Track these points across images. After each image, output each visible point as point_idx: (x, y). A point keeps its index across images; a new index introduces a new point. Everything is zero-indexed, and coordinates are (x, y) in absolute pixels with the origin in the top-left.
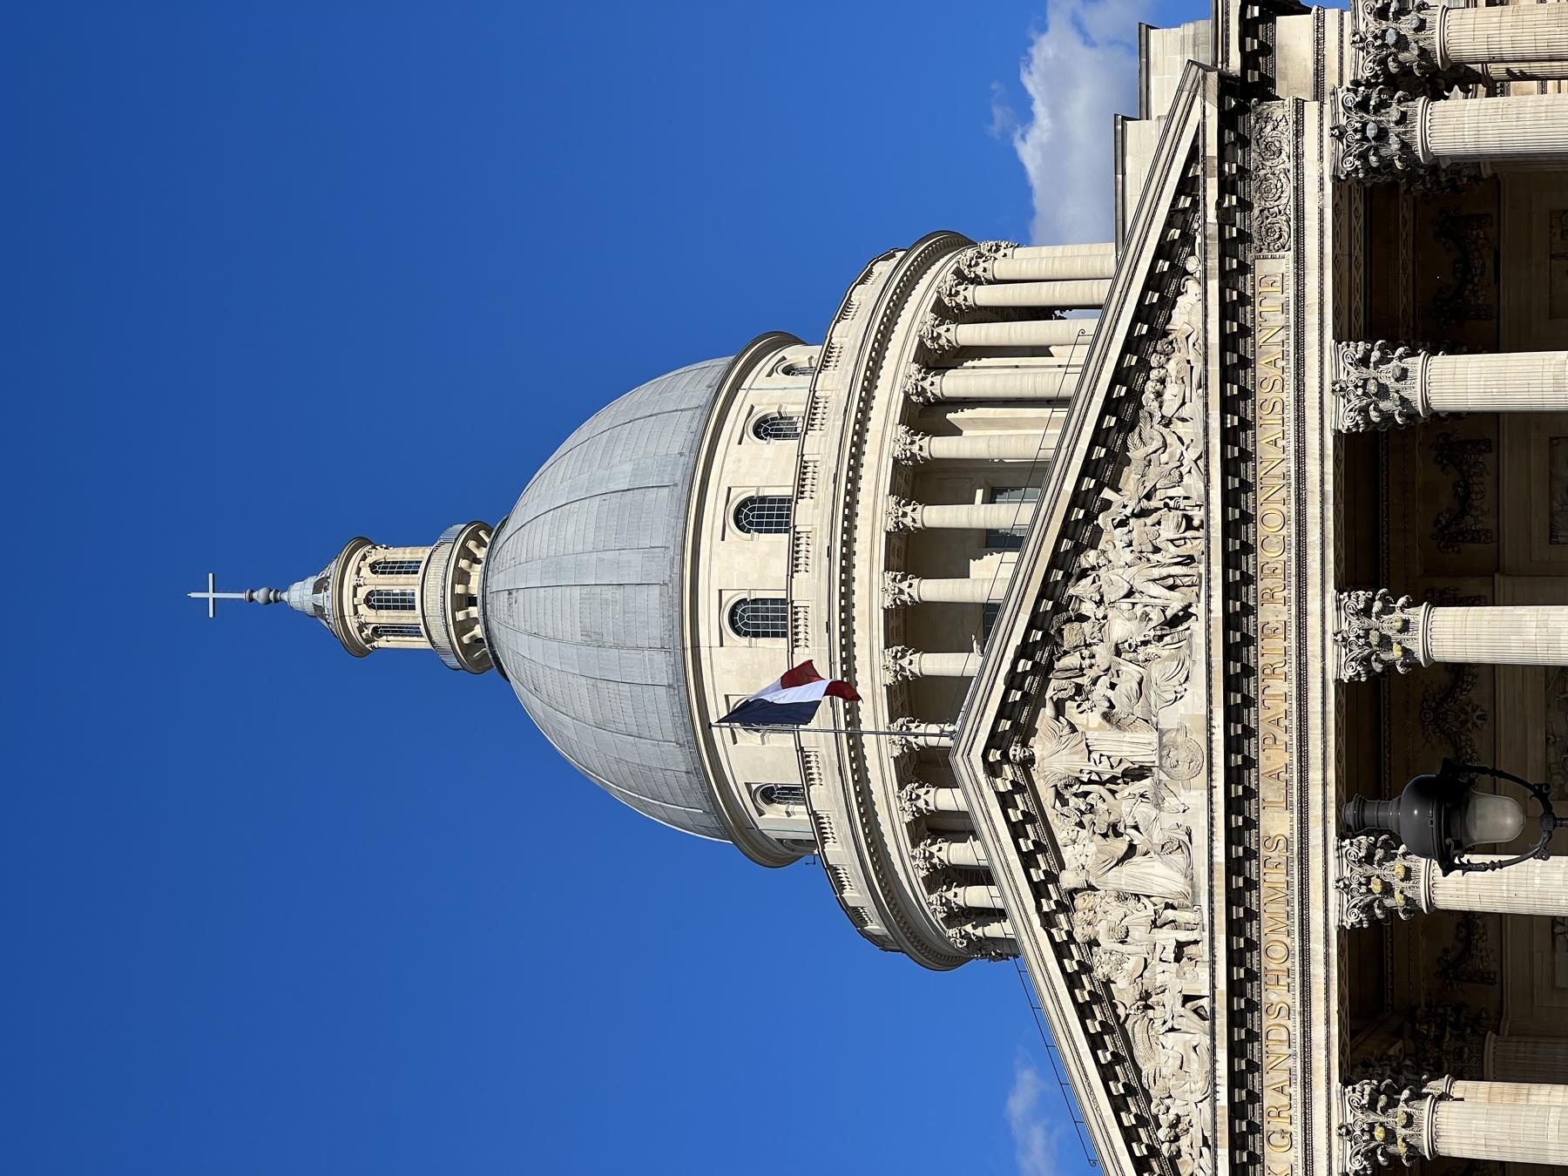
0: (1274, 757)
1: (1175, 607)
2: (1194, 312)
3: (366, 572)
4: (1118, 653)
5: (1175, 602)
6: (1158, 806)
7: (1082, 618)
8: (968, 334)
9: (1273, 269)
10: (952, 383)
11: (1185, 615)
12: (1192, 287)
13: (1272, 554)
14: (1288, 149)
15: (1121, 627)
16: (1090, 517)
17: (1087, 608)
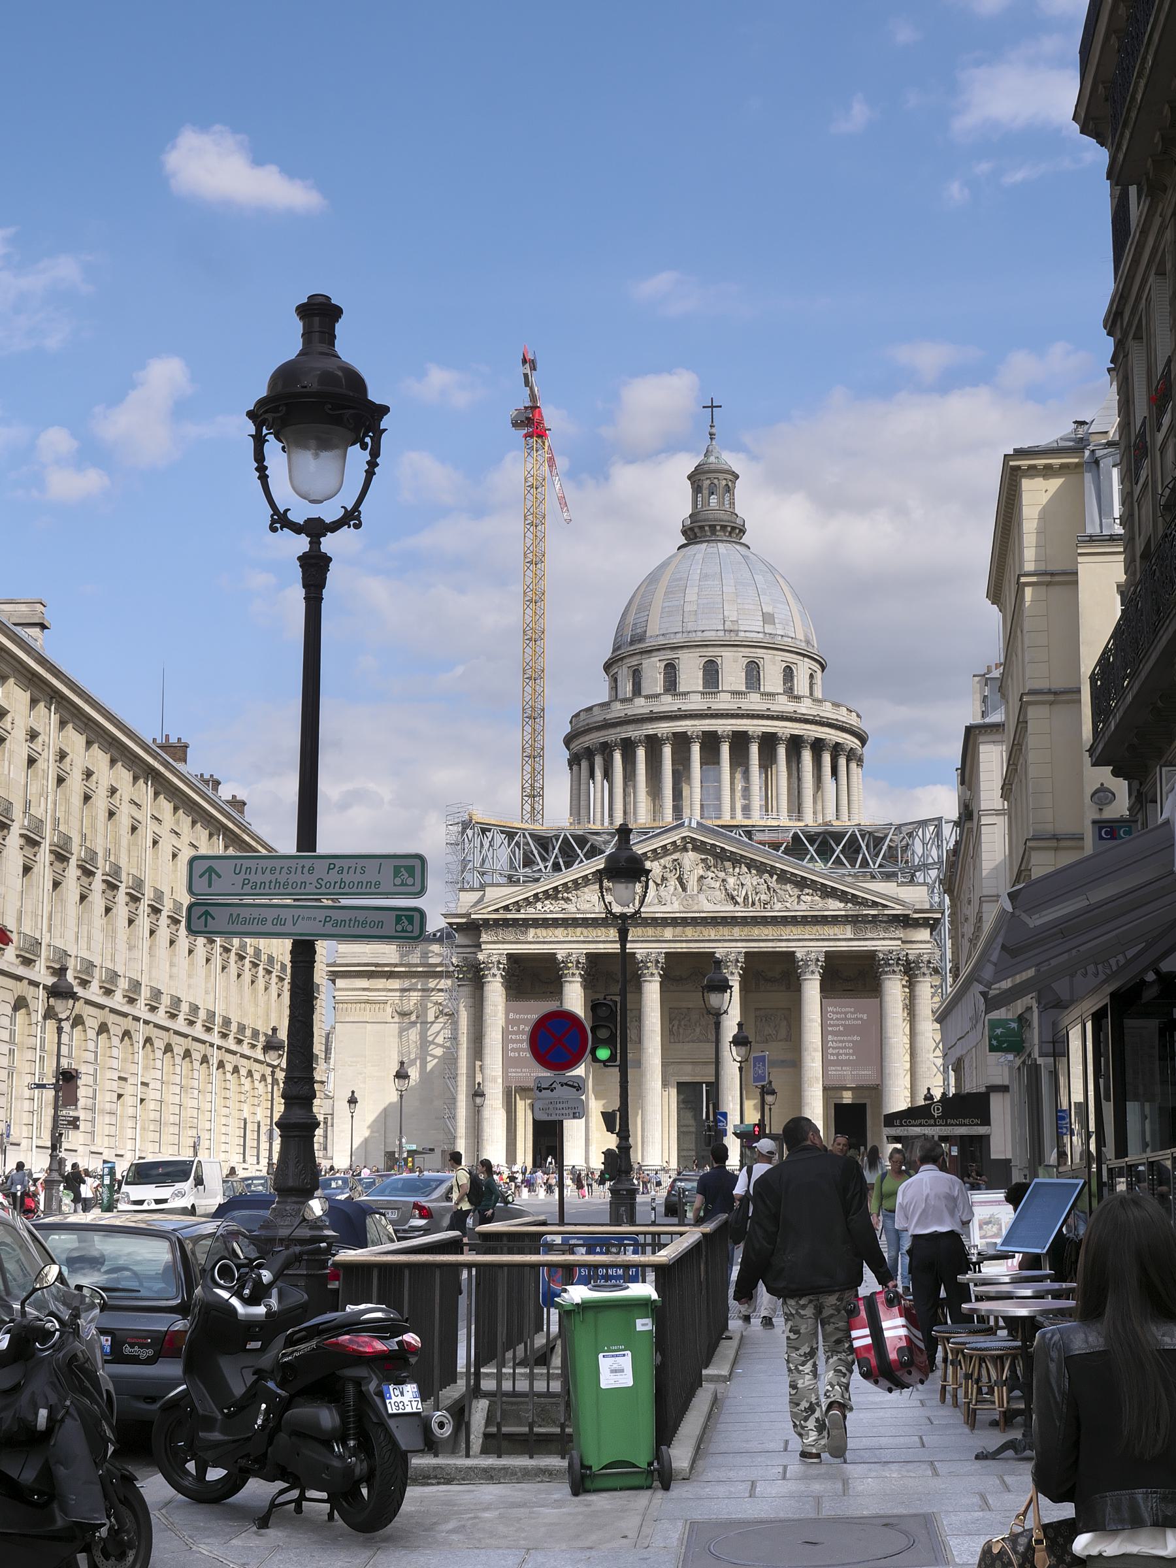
0: (690, 932)
1: (739, 900)
2: (835, 907)
3: (724, 482)
4: (723, 880)
5: (740, 900)
6: (673, 894)
7: (734, 868)
8: (827, 758)
9: (848, 932)
10: (807, 756)
11: (736, 903)
12: (842, 905)
13: (756, 932)
14: (887, 935)
15: (731, 881)
16: (767, 872)
17: (737, 870)
